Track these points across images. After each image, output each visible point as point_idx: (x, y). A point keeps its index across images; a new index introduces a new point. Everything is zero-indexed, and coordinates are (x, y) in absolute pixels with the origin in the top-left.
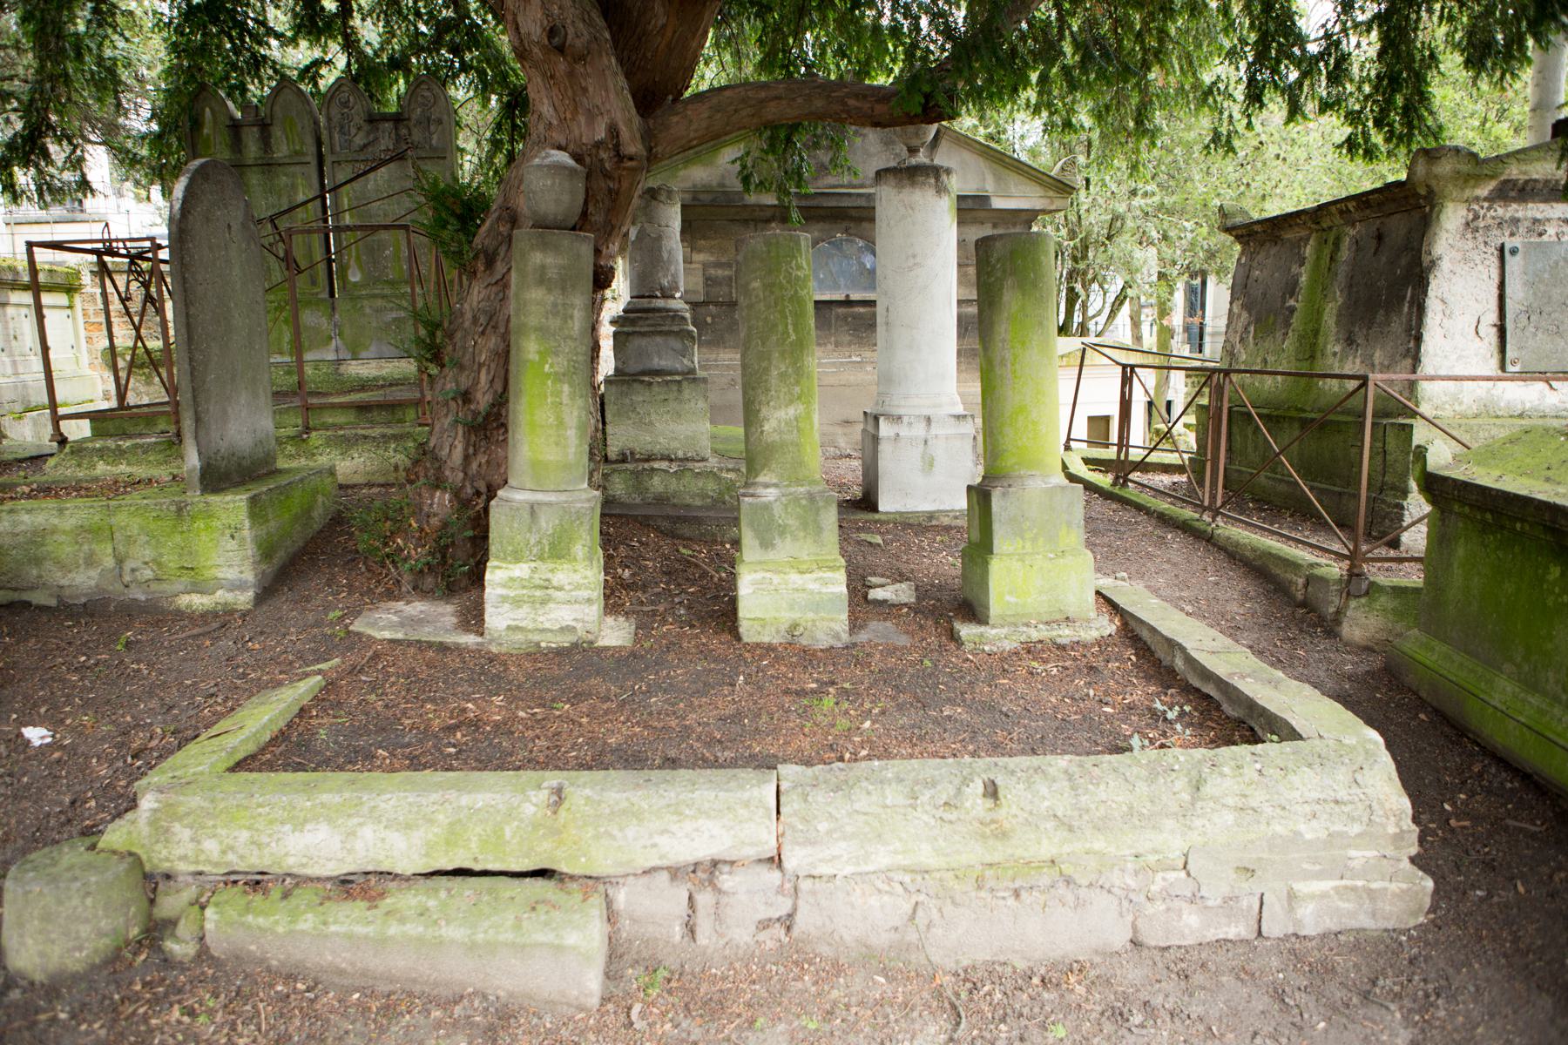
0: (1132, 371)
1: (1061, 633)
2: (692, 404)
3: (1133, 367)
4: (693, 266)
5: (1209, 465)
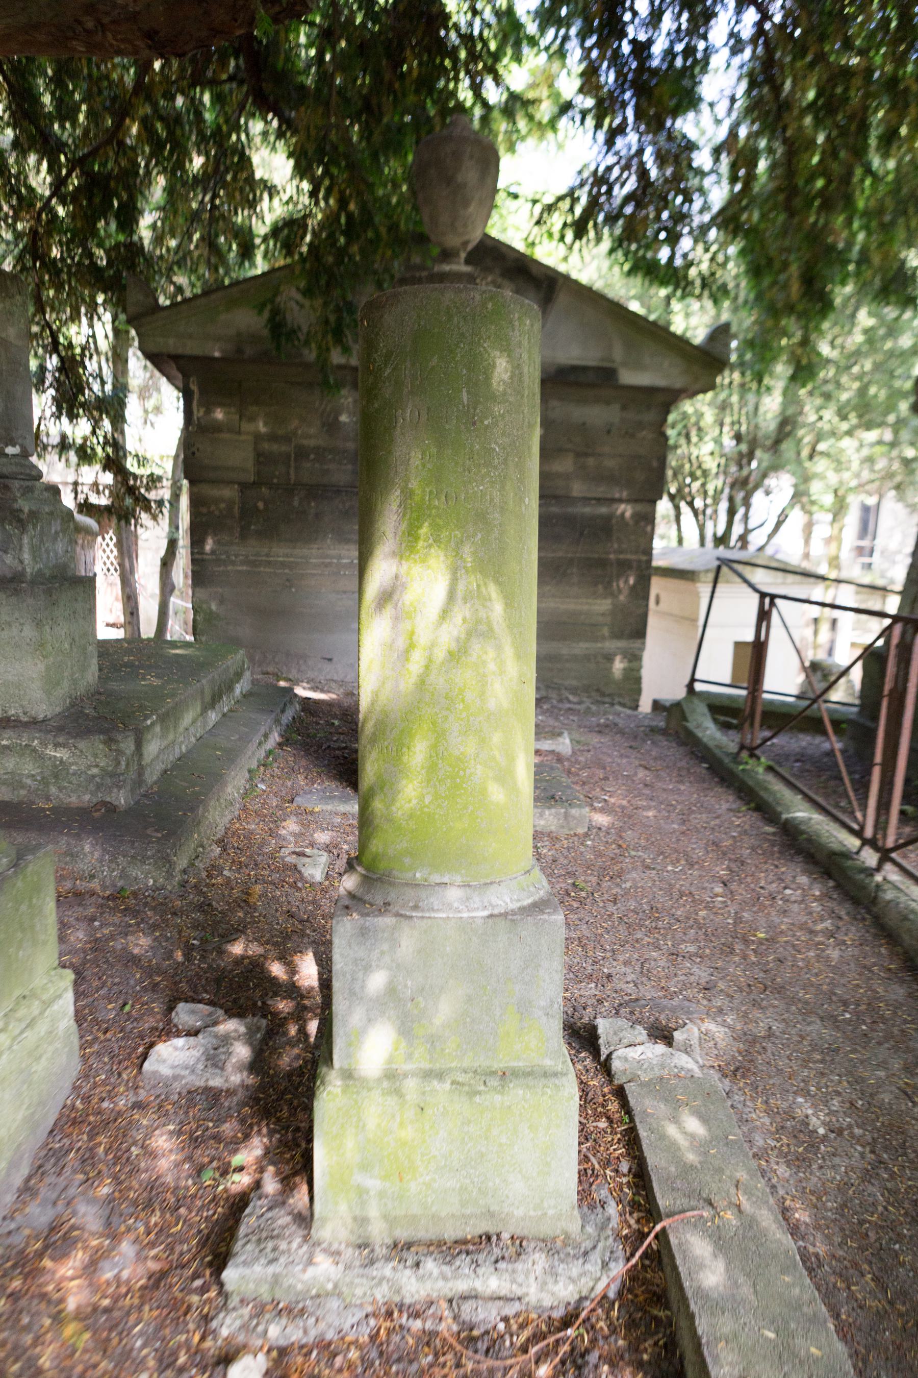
0: (772, 604)
1: (478, 1285)
2: (15, 631)
3: (773, 597)
4: (243, 437)
5: (876, 774)
